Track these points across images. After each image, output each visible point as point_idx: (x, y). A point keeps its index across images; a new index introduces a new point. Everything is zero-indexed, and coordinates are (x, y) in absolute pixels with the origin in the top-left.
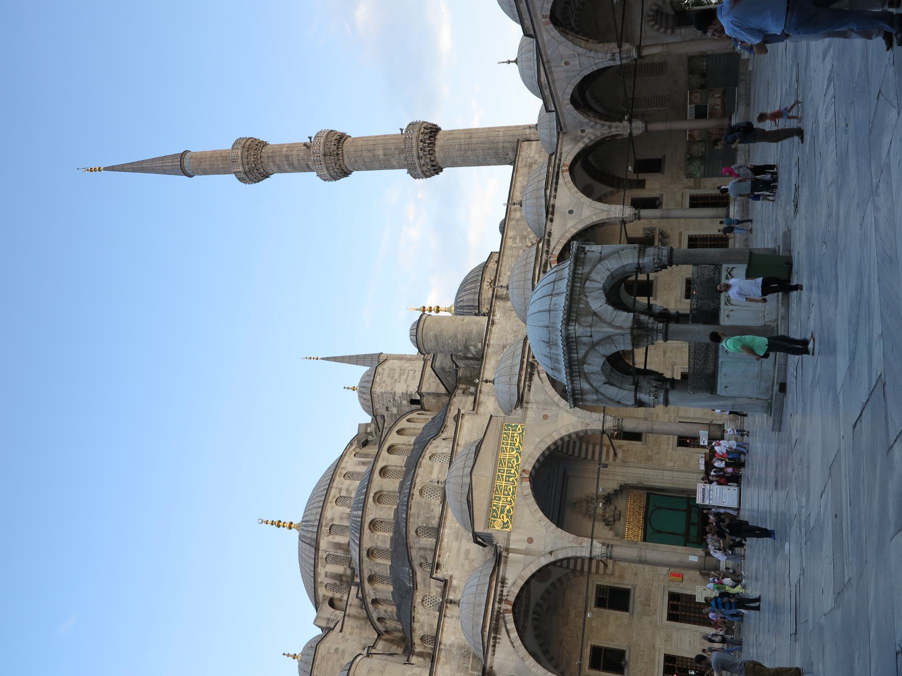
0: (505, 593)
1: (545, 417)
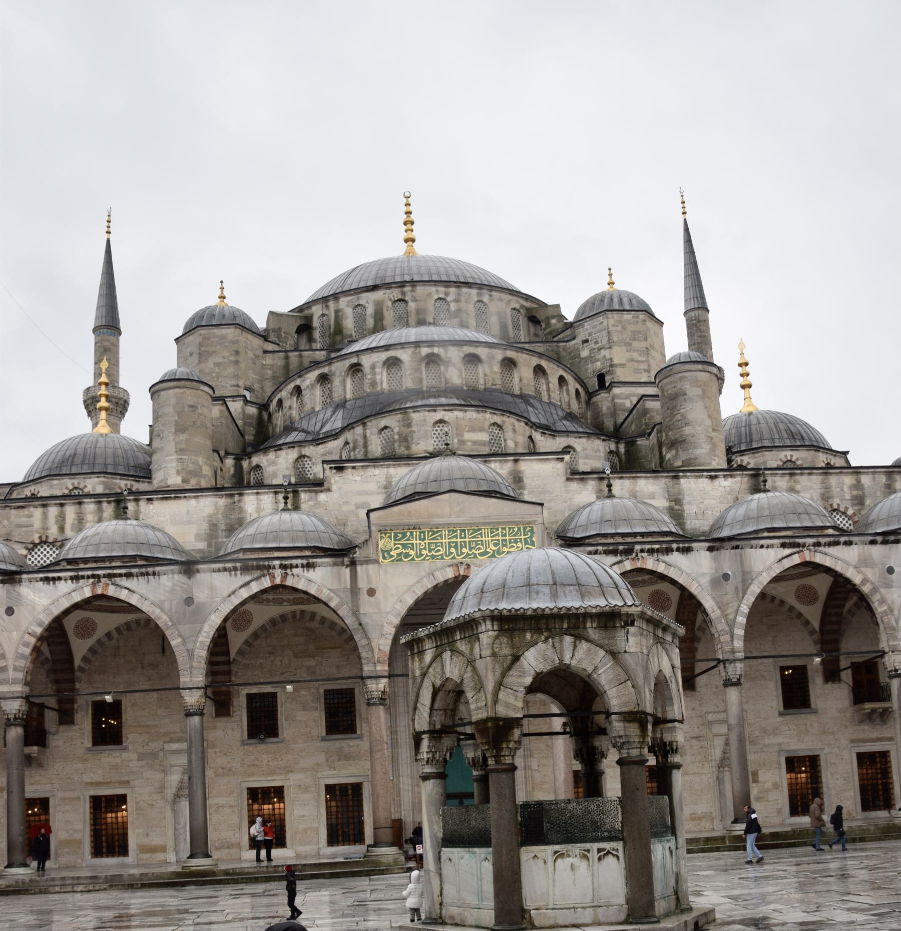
0: (295, 571)
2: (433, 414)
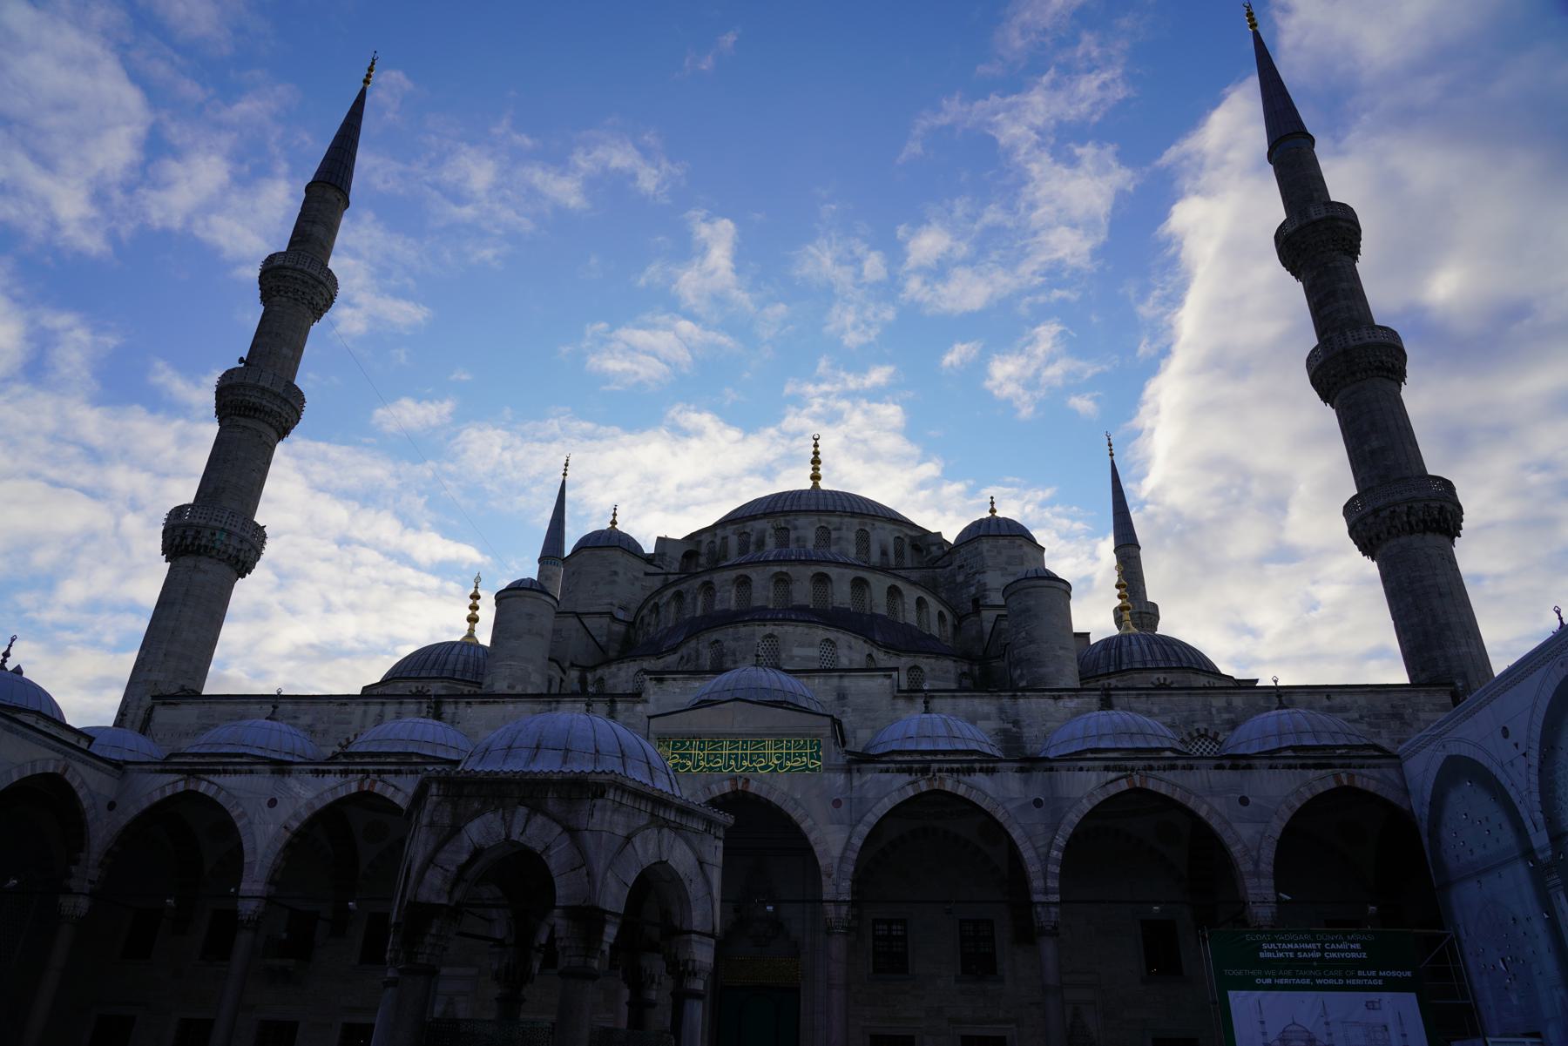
1: (837, 803)
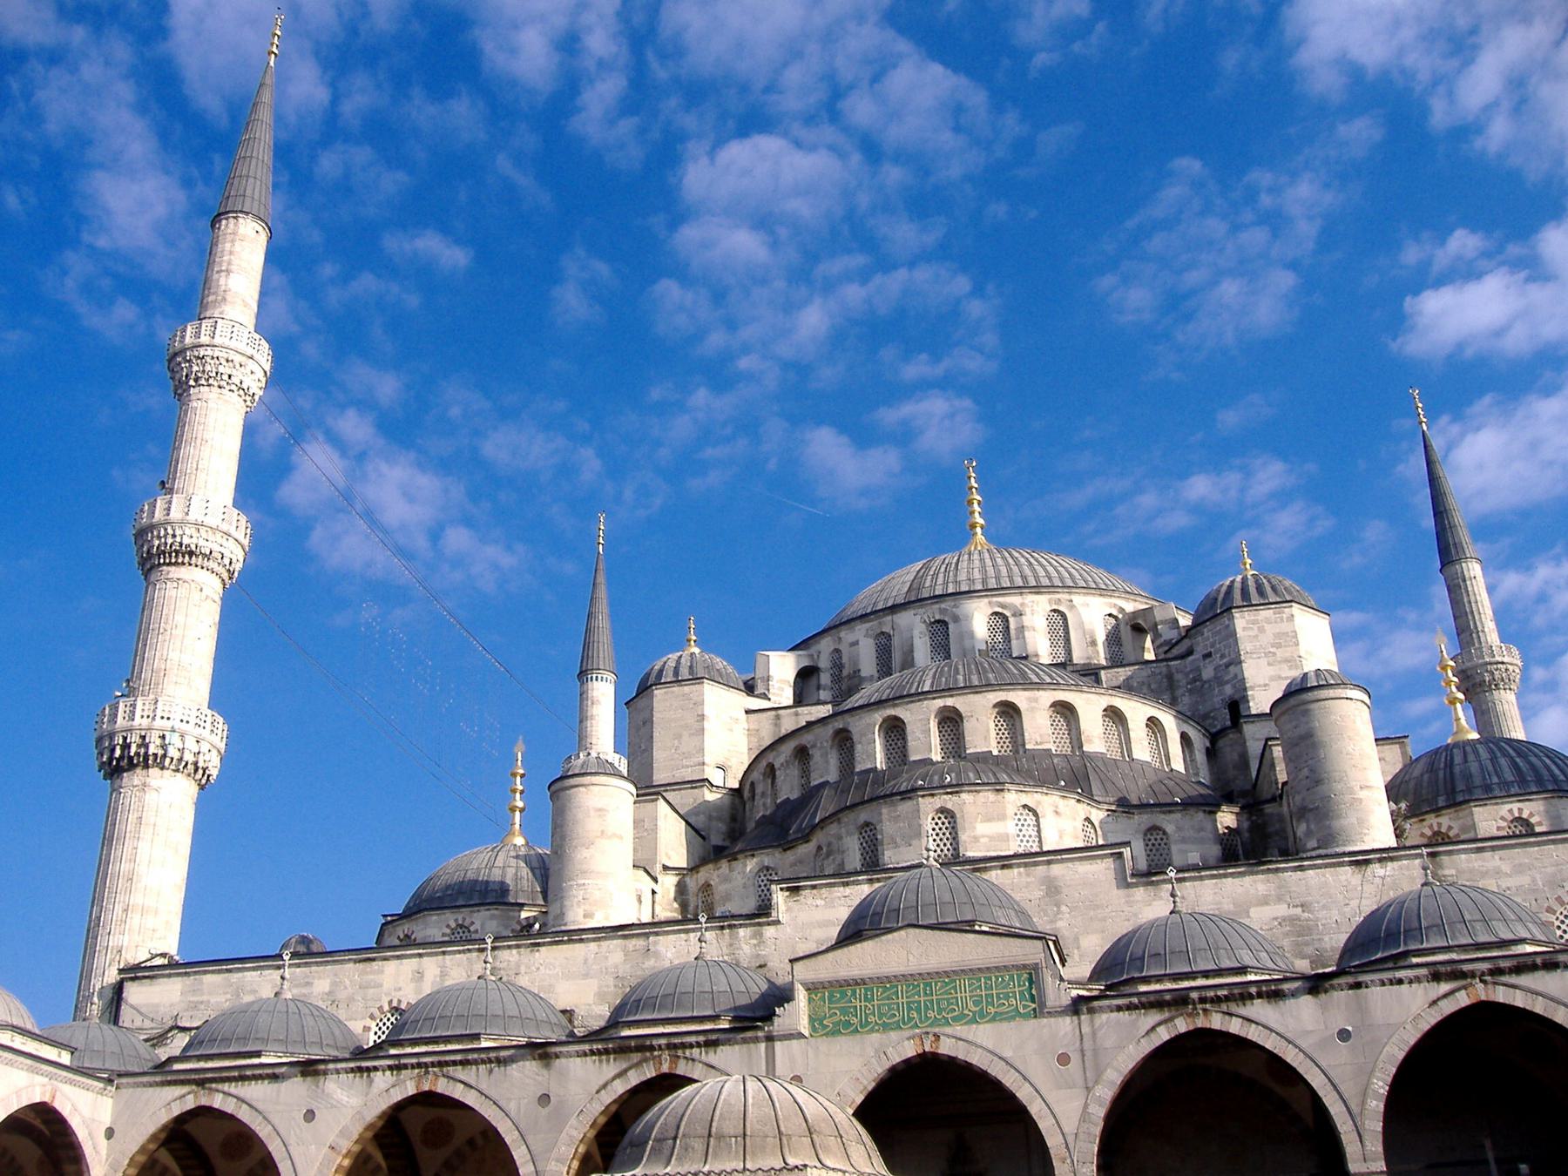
1: (1064, 1059)
2: (930, 799)
